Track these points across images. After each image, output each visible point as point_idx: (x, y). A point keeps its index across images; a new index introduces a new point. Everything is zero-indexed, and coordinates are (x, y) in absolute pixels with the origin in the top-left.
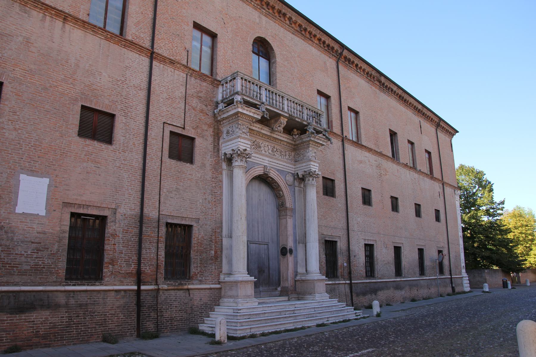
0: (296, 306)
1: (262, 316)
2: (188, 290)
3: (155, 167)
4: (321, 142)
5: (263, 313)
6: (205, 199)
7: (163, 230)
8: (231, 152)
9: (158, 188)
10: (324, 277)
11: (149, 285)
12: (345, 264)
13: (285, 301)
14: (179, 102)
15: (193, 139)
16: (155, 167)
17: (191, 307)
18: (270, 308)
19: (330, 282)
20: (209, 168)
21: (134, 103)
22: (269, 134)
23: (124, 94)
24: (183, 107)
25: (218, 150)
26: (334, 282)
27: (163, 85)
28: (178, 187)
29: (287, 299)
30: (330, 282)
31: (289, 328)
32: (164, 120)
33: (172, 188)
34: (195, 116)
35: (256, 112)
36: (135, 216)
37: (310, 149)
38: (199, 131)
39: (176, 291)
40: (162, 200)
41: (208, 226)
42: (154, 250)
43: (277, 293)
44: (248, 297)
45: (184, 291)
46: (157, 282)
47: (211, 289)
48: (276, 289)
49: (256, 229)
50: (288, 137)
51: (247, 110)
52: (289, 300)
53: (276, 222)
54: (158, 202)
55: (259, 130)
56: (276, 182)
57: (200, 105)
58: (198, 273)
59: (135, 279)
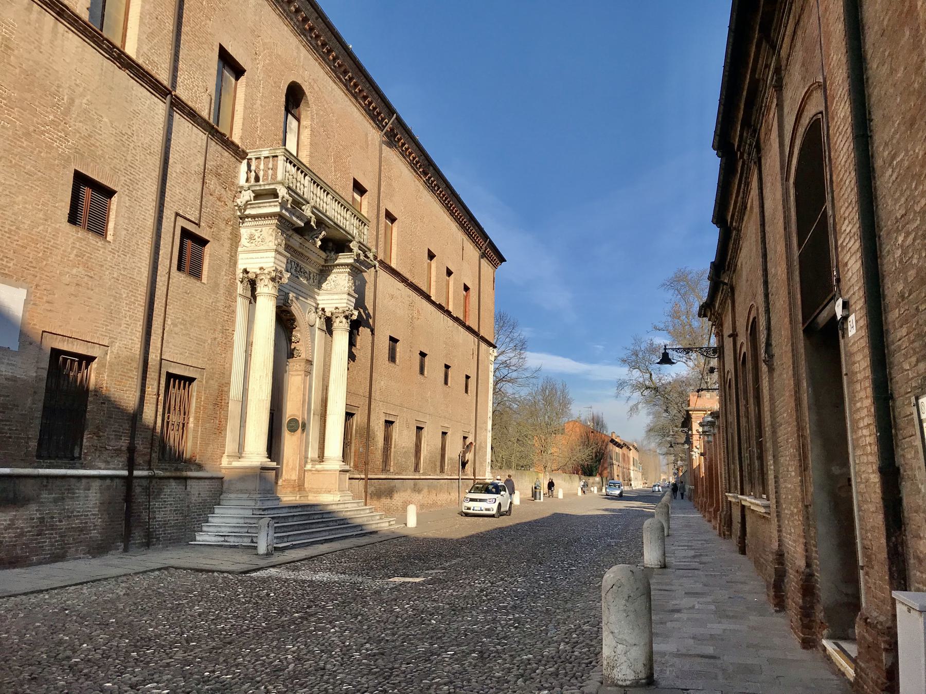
2: (186, 479)
6: (215, 339)
8: (258, 272)
15: (203, 242)
23: (129, 158)
24: (200, 189)
25: (235, 263)
46: (150, 465)
54: (160, 340)
57: (219, 188)
59: (124, 458)
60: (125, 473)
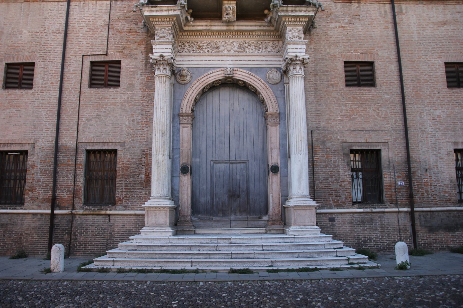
0: (232, 241)
1: (156, 249)
2: (109, 215)
3: (74, 99)
4: (302, 14)
5: (158, 246)
6: (133, 121)
7: (82, 158)
9: (77, 118)
10: (314, 203)
11: (65, 209)
12: (401, 183)
13: (260, 233)
14: (101, 31)
15: (119, 63)
16: (74, 99)
17: (111, 233)
18: (181, 241)
19: (361, 210)
20: (138, 88)
21: (52, 47)
22: (225, 28)
26: (369, 210)
27: (83, 20)
28: (99, 113)
29: (264, 231)
30: (361, 210)
31: (167, 268)
32: (84, 53)
33: (92, 116)
34: (121, 38)
35: (170, 8)
36: (53, 148)
37: (288, 28)
38: (125, 52)
39: (94, 216)
40: (81, 128)
41: (136, 149)
42: (71, 177)
43: (261, 223)
44: (160, 225)
45: (104, 216)
47: (135, 215)
48: (260, 218)
49: (227, 145)
50: (259, 24)
51: (157, 11)
52: (266, 233)
53: (261, 134)
54: (76, 132)
55: (208, 28)
56: (250, 85)
57: (127, 25)
58: (123, 198)
60: (49, 212)
